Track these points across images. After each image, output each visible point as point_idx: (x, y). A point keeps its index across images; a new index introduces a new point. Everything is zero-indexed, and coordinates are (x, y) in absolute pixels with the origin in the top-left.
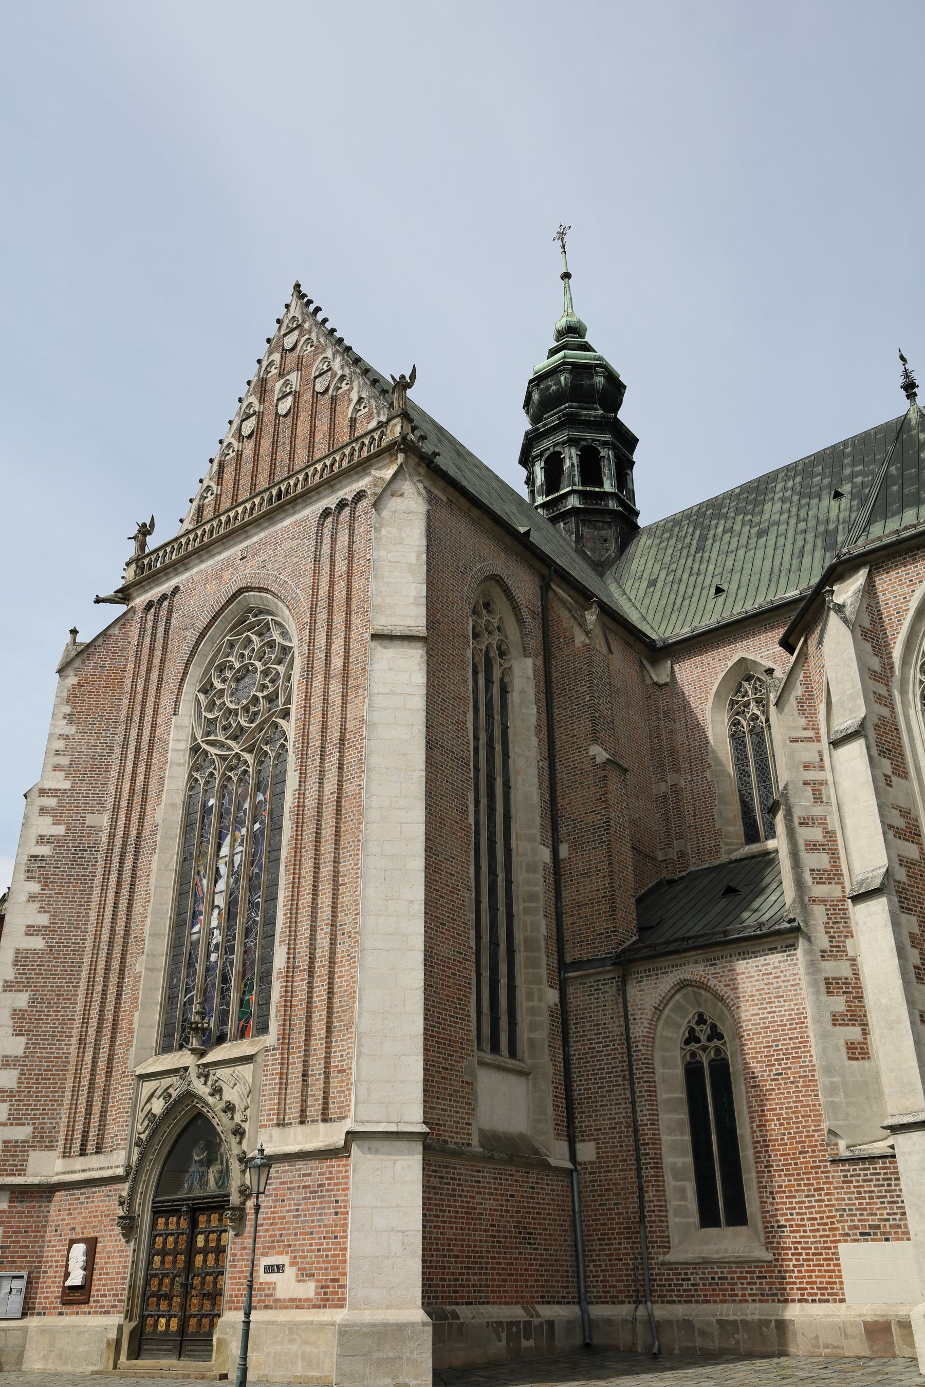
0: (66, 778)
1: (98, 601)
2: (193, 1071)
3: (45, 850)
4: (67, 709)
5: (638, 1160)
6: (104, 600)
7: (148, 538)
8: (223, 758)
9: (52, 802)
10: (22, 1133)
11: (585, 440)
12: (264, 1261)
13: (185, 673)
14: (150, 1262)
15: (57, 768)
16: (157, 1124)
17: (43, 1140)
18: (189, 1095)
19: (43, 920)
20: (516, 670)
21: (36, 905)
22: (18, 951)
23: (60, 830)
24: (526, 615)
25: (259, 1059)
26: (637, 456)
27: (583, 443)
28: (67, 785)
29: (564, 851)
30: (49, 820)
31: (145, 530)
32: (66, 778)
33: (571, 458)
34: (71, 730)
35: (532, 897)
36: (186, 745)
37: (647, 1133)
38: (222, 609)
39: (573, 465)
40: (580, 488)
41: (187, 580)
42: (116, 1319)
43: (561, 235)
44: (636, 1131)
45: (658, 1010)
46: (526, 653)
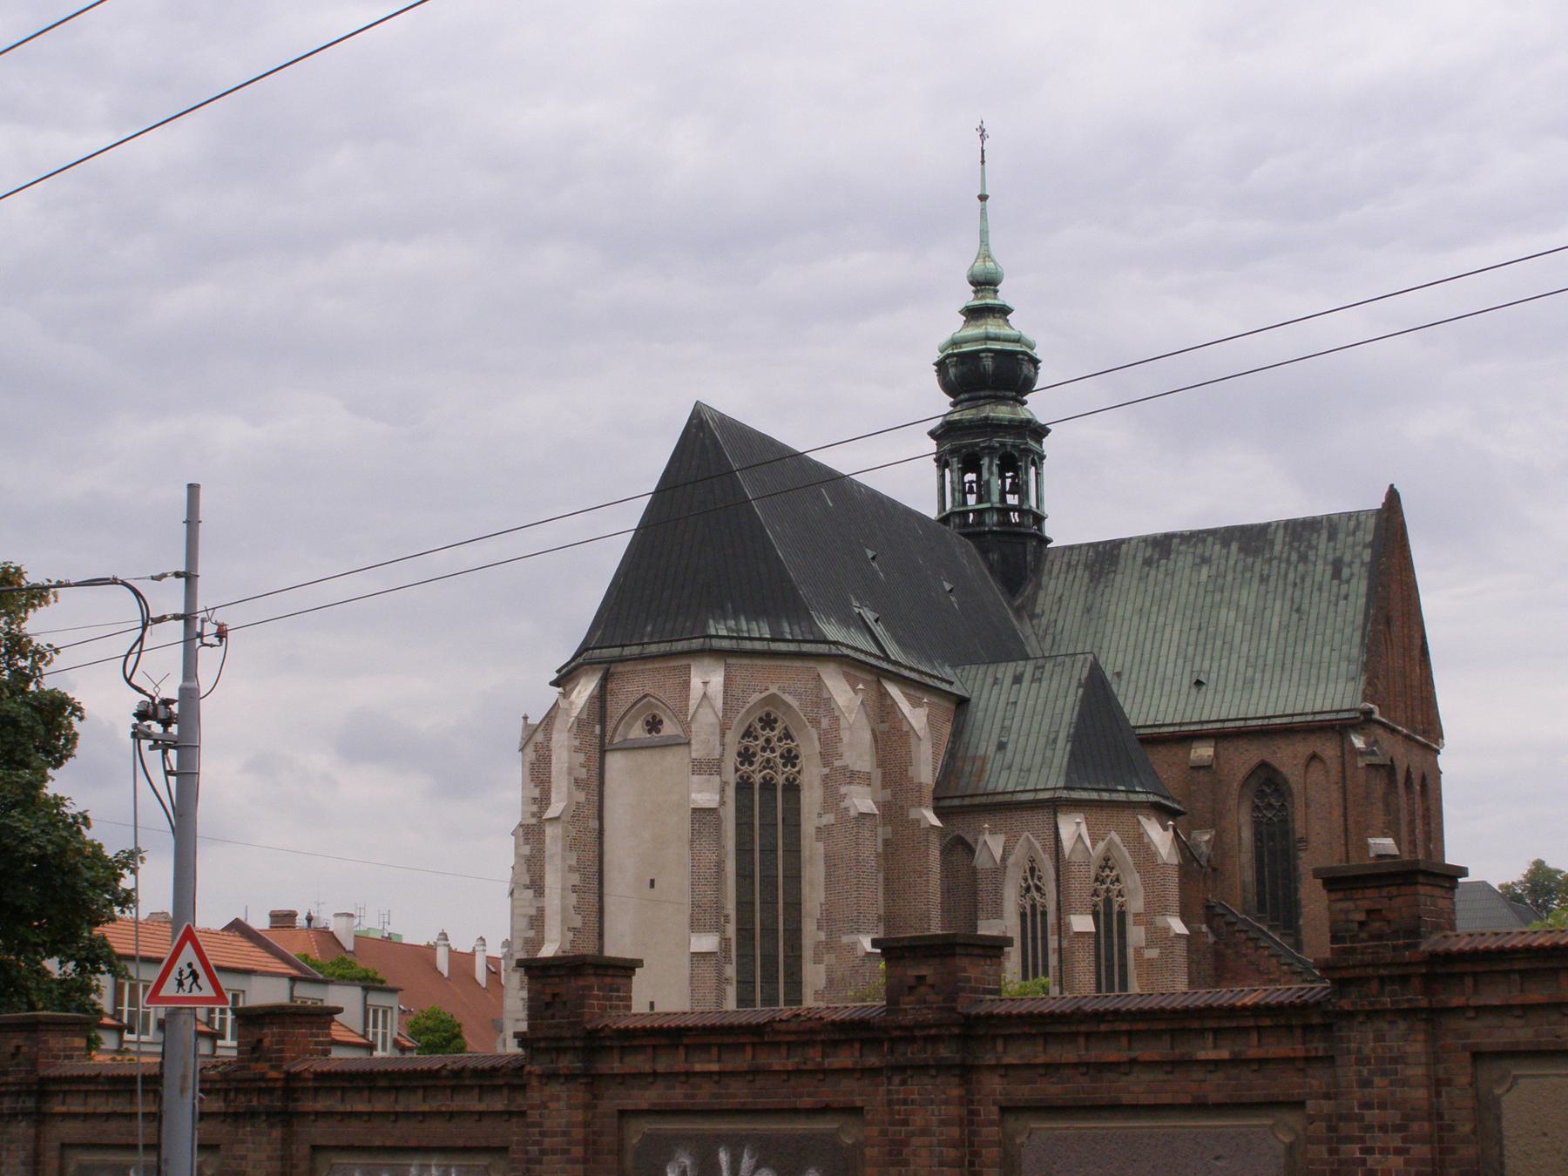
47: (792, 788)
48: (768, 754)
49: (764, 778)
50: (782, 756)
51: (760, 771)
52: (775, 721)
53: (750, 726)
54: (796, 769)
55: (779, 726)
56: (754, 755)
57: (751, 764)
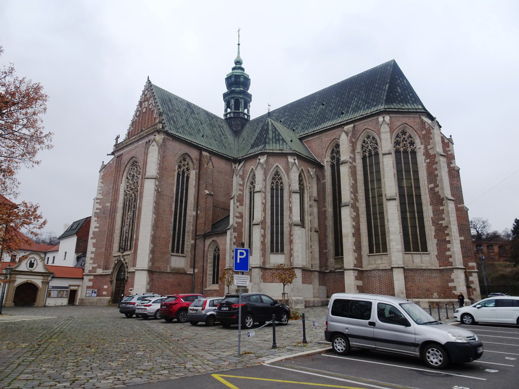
0: (102, 196)
1: (108, 155)
2: (121, 256)
3: (98, 211)
4: (101, 181)
5: (203, 272)
6: (109, 155)
7: (118, 139)
8: (129, 194)
9: (99, 201)
10: (95, 265)
11: (236, 97)
12: (130, 289)
13: (123, 174)
14: (116, 288)
15: (100, 193)
16: (116, 264)
17: (99, 267)
18: (120, 260)
19: (98, 225)
20: (191, 173)
21: (96, 222)
22: (93, 231)
23: (101, 207)
24: (194, 161)
25: (131, 255)
27: (235, 98)
28: (102, 197)
29: (199, 212)
30: (98, 205)
31: (118, 138)
32: (102, 196)
33: (232, 103)
34: (102, 185)
35: (190, 222)
36: (123, 190)
37: (205, 268)
38: (129, 161)
39: (232, 104)
40: (233, 111)
41: (124, 152)
42: (110, 298)
44: (203, 267)
45: (209, 245)
46: (194, 169)
47: (414, 153)
48: (404, 142)
49: (404, 149)
50: (409, 143)
51: (402, 148)
52: (406, 133)
53: (398, 134)
54: (414, 147)
55: (407, 134)
56: (400, 143)
57: (399, 145)
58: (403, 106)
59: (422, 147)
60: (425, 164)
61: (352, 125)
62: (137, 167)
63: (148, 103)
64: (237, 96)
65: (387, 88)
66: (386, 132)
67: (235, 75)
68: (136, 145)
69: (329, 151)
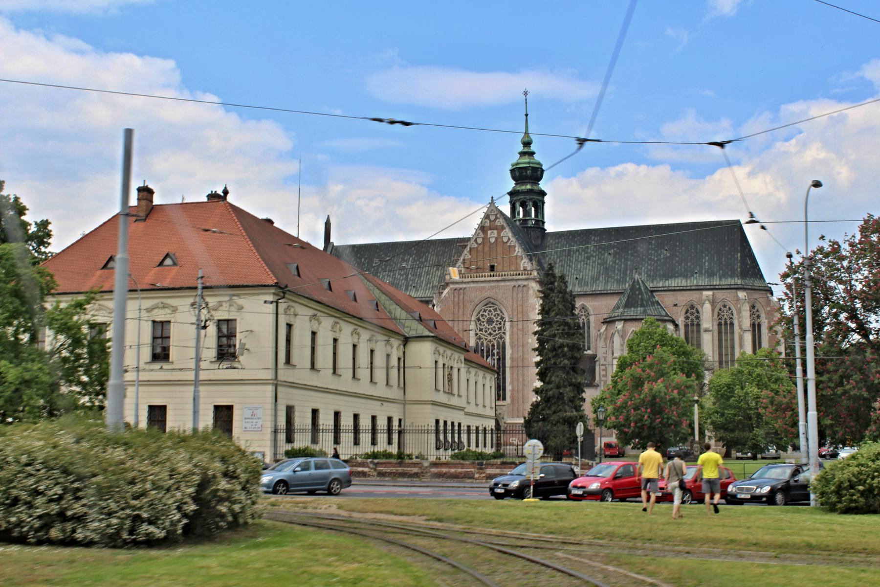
8: (486, 339)
26: (546, 199)
43: (526, 93)
55: (756, 308)
58: (754, 281)
59: (766, 321)
60: (767, 337)
61: (710, 293)
62: (495, 310)
63: (499, 234)
64: (535, 197)
65: (739, 258)
66: (746, 310)
67: (533, 168)
68: (492, 284)
69: (684, 311)
